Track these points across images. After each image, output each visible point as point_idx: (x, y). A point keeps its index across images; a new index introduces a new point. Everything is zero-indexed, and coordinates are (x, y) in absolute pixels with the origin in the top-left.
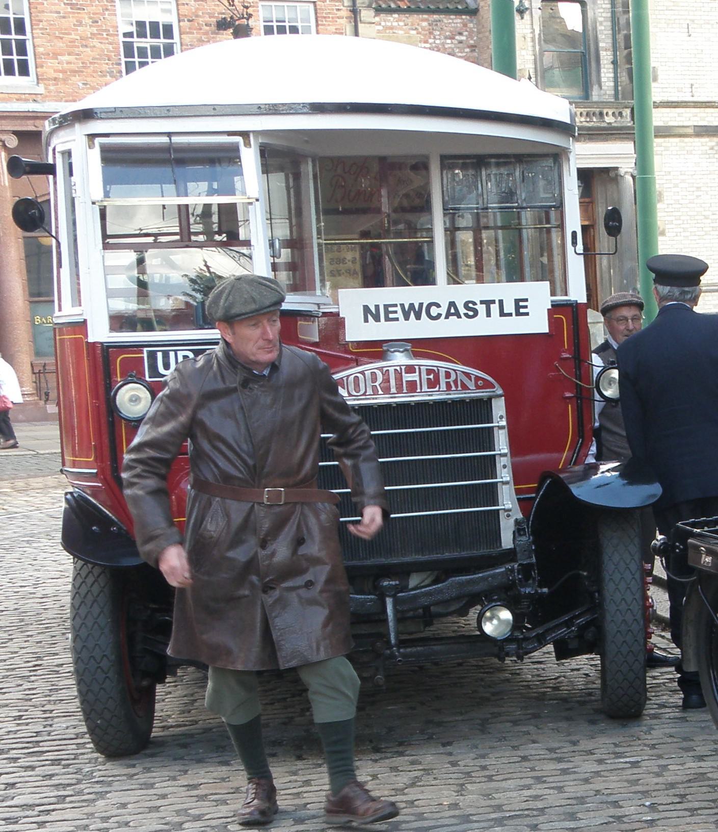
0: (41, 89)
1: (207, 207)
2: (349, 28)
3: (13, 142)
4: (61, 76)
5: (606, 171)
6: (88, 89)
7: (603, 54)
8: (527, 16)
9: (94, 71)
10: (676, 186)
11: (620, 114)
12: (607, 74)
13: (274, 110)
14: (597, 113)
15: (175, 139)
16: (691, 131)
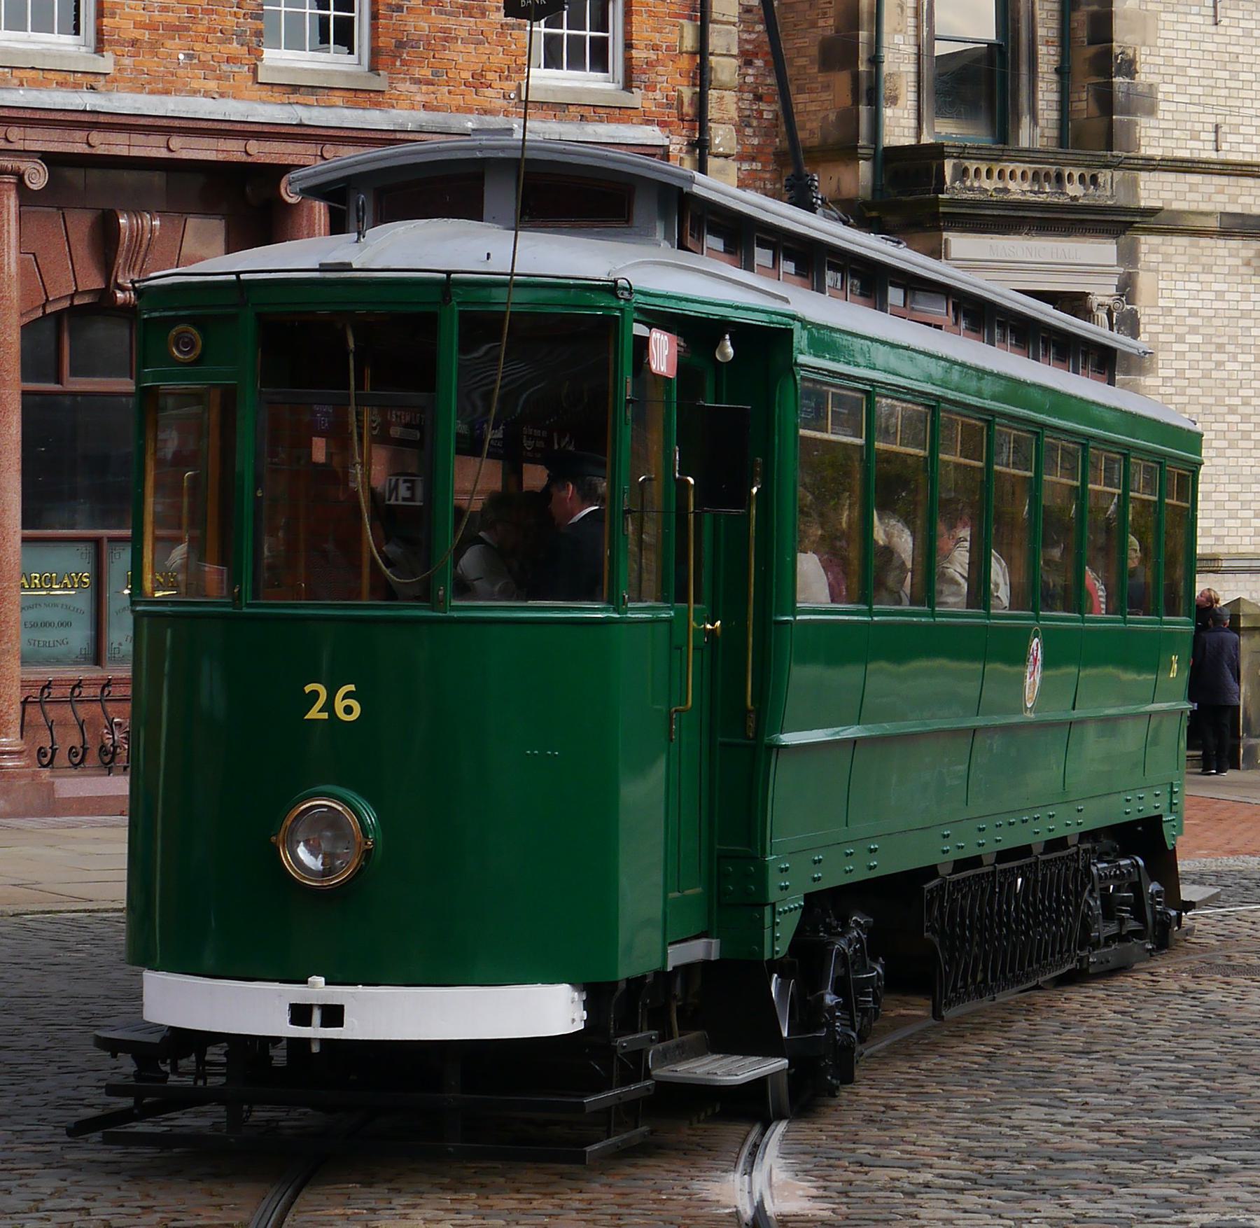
0: (106, 63)
3: (38, 178)
6: (193, 67)
7: (1042, 50)
9: (210, 30)
10: (1180, 339)
11: (1094, 179)
12: (1047, 95)
14: (1053, 174)
16: (1213, 223)
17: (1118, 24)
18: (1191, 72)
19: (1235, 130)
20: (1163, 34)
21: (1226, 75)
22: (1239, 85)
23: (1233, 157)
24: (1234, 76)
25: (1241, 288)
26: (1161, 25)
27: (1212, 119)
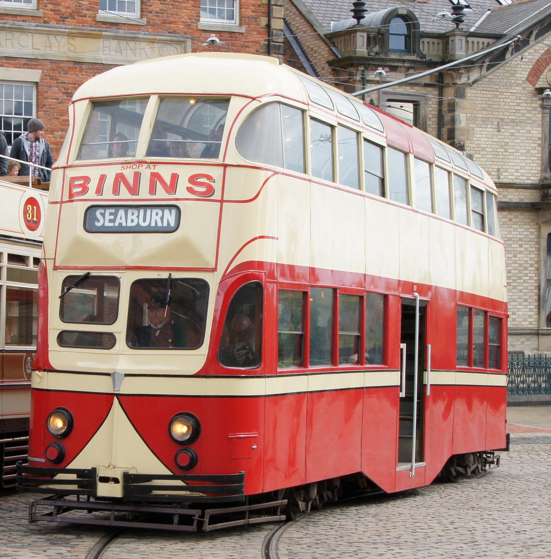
4: (55, 146)
17: (457, 133)
18: (487, 149)
19: (506, 171)
20: (476, 135)
21: (503, 150)
22: (508, 154)
23: (505, 181)
24: (506, 151)
25: (508, 229)
26: (475, 132)
27: (496, 167)
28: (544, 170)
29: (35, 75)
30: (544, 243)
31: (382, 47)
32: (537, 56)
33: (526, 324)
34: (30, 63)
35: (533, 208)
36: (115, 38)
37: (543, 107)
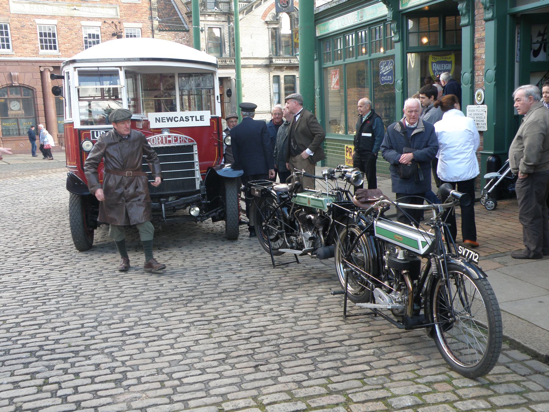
0: (60, 54)
1: (109, 89)
2: (151, 36)
3: (52, 69)
5: (227, 78)
7: (226, 43)
8: (204, 32)
12: (227, 49)
13: (129, 60)
15: (100, 69)
28: (270, 52)
29: (55, 22)
30: (272, 79)
31: (204, 7)
32: (265, 9)
33: (266, 110)
34: (53, 17)
35: (267, 66)
36: (87, 6)
37: (268, 28)
